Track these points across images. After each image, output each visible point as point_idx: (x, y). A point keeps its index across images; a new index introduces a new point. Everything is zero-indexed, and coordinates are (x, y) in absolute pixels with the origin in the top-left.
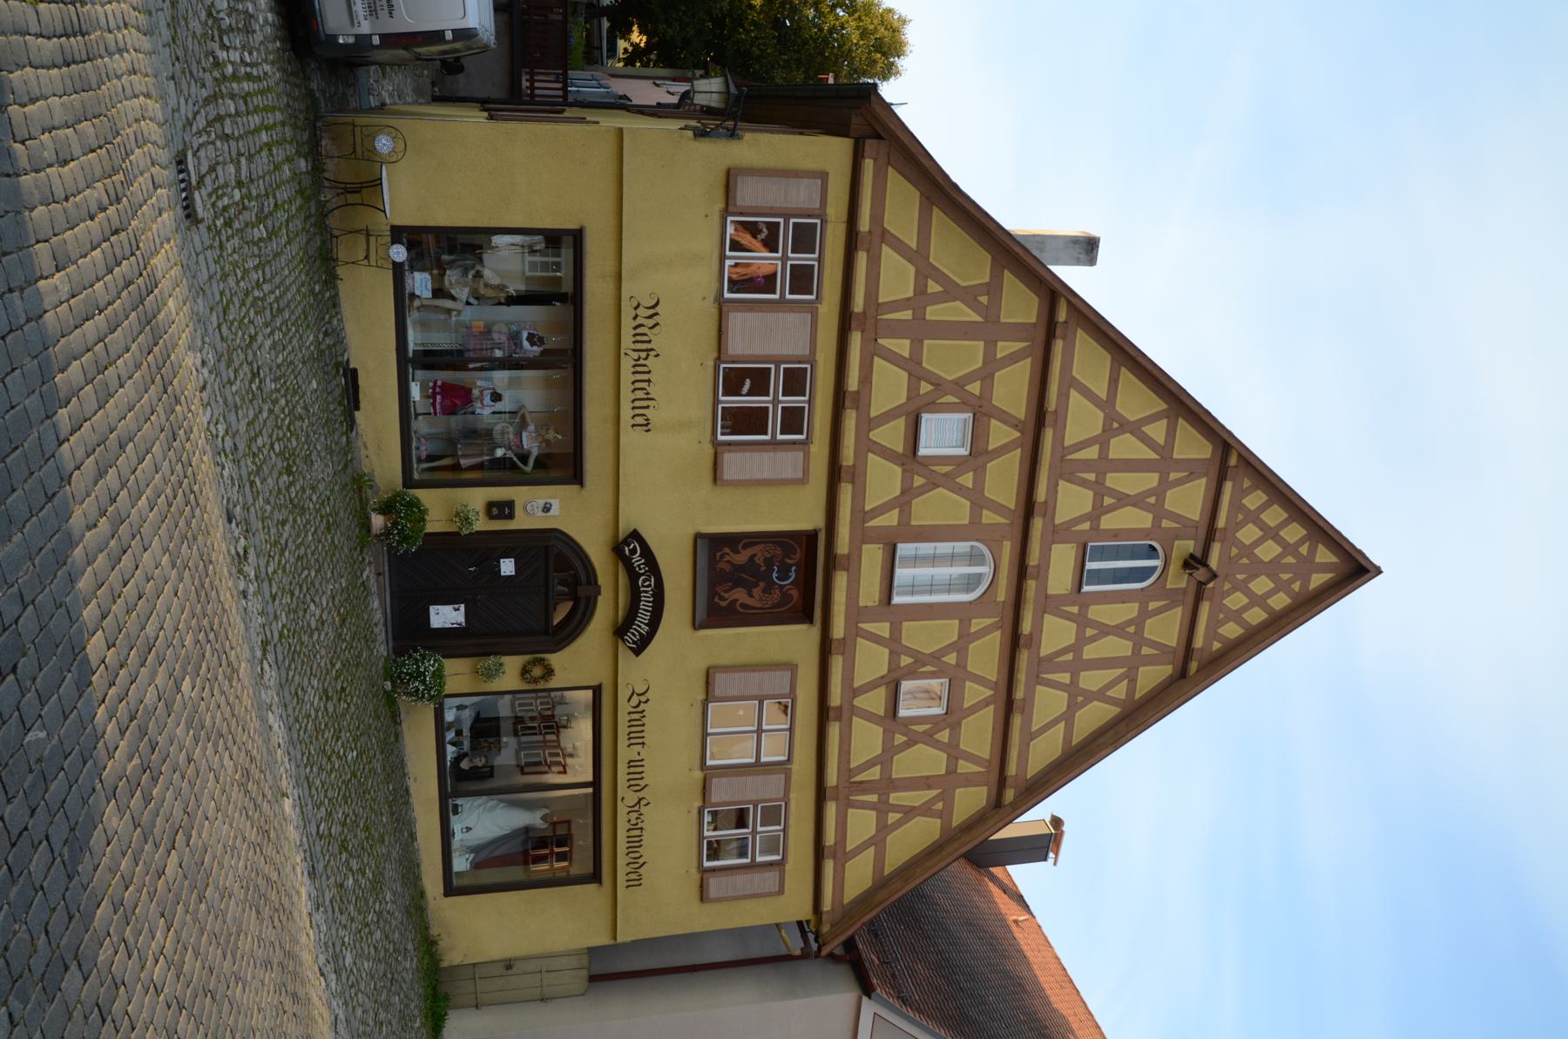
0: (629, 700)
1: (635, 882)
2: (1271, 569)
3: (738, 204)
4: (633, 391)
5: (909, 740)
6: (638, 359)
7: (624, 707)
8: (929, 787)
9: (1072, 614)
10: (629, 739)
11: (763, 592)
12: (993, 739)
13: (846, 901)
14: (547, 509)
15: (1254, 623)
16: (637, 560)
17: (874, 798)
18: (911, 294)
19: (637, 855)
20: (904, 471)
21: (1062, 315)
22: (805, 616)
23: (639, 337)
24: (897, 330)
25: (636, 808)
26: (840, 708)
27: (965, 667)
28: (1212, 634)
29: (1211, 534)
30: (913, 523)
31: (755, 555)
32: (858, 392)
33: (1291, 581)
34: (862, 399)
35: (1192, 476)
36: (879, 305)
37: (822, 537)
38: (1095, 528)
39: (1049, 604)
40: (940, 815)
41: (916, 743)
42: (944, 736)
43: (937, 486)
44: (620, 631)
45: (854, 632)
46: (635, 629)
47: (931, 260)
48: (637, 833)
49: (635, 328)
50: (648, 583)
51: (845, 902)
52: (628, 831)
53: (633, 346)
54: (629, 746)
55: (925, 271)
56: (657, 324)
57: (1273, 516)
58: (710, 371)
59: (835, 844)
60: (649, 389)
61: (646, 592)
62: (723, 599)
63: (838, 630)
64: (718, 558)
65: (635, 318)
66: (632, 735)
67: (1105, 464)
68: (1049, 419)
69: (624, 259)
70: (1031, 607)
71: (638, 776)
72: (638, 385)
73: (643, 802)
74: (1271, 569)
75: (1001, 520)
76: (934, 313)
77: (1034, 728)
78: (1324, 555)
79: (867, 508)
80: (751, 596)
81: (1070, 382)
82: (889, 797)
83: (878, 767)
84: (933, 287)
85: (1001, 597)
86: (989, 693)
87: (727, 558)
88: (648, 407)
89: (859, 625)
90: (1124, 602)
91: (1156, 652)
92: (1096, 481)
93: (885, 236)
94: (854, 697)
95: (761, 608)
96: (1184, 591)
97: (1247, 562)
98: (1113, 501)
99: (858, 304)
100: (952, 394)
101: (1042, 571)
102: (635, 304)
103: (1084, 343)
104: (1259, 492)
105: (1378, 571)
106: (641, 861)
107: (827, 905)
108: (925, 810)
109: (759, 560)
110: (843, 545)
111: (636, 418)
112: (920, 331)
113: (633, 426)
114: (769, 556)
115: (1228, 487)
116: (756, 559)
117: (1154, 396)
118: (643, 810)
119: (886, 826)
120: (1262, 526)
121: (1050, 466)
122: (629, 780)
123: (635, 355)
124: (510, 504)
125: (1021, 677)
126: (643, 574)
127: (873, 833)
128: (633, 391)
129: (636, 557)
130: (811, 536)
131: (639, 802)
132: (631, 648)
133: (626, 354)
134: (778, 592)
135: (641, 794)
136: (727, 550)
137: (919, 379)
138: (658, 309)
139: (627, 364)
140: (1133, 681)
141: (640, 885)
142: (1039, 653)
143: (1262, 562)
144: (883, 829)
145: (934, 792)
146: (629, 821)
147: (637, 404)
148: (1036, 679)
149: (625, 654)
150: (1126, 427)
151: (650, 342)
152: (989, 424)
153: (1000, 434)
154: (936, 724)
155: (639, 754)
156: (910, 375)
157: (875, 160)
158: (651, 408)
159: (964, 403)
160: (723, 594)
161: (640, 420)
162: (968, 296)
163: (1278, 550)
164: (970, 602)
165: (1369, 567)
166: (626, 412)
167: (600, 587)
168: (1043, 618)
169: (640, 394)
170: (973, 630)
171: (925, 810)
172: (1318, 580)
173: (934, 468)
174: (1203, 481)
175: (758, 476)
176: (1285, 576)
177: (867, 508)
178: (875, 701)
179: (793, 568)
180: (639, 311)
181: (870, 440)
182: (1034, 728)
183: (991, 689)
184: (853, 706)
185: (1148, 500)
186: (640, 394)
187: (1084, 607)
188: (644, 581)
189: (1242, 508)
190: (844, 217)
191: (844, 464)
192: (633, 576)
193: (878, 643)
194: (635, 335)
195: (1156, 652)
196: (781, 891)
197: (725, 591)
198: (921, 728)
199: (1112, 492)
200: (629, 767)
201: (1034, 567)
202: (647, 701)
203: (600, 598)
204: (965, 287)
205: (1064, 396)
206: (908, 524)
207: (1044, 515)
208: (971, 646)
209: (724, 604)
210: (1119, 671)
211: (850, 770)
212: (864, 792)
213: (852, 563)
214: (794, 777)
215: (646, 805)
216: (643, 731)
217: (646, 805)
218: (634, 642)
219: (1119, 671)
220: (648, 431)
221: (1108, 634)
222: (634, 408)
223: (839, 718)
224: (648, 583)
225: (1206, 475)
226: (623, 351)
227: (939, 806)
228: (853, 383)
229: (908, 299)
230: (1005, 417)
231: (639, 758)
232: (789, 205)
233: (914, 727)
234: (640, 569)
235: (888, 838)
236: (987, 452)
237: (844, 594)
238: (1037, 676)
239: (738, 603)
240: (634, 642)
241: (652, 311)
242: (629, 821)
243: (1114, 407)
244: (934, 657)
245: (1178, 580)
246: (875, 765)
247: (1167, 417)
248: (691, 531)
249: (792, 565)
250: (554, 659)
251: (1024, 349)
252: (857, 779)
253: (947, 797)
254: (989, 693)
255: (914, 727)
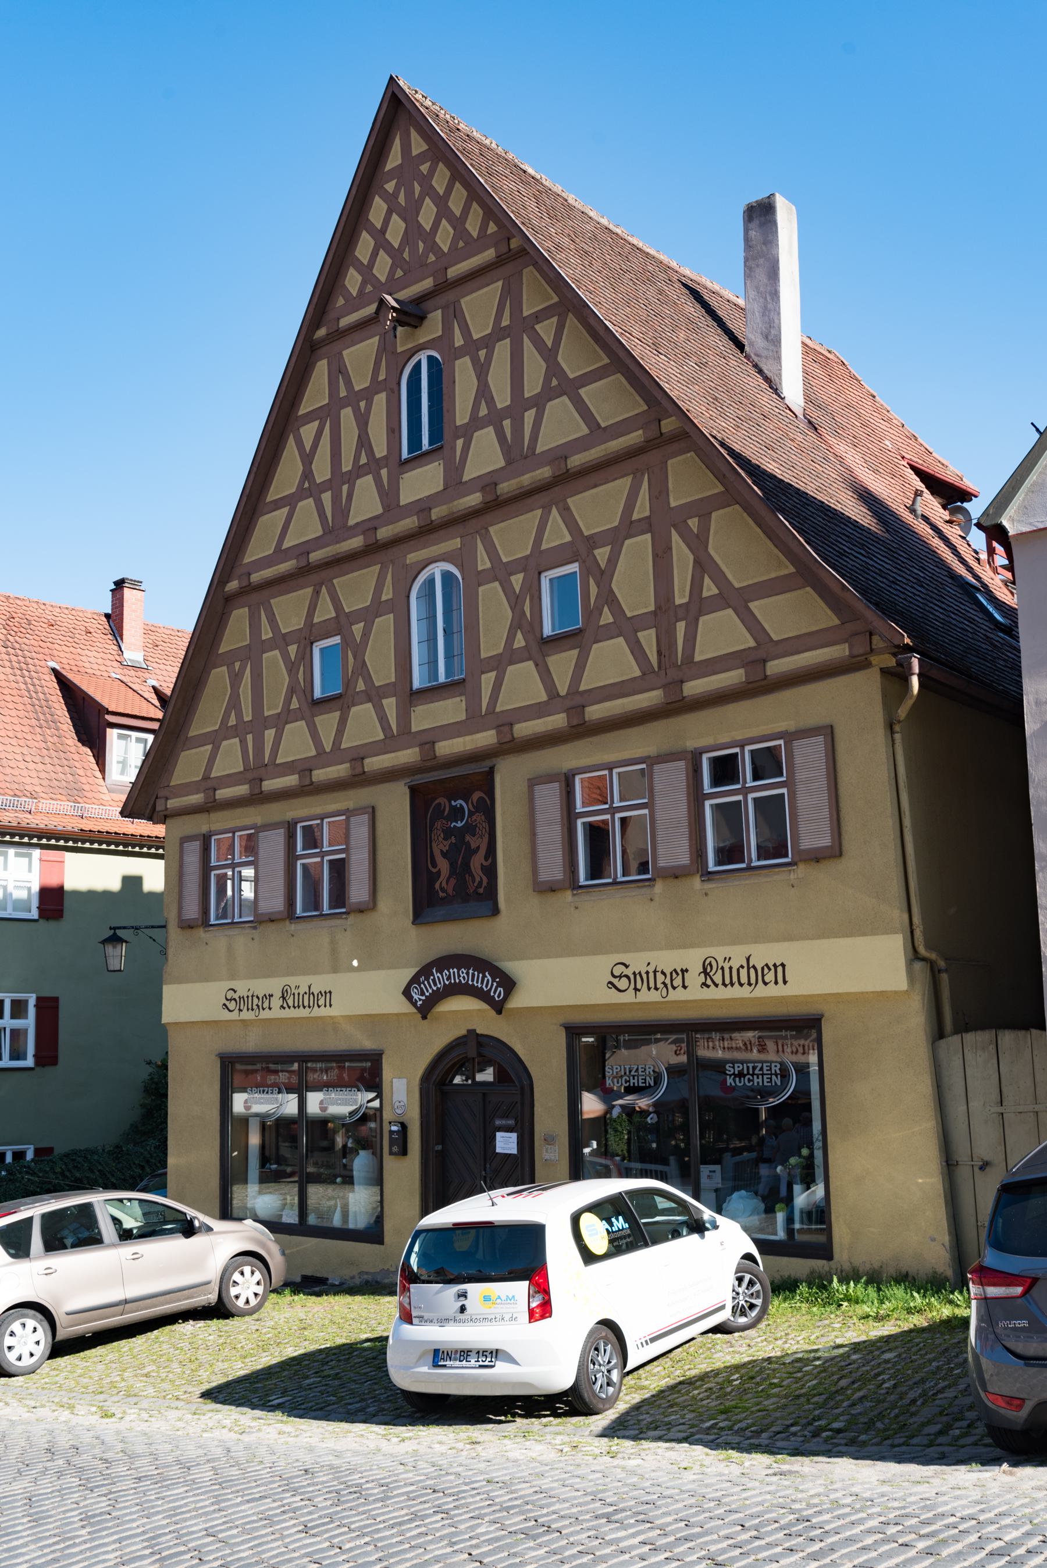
20: (354, 705)
36: (245, 770)
37: (420, 779)
62: (481, 882)
63: (486, 738)
80: (478, 848)
81: (280, 554)
82: (680, 605)
85: (456, 543)
87: (444, 884)
93: (206, 778)
96: (444, 308)
108: (698, 543)
110: (408, 756)
121: (338, 542)
134: (474, 817)
145: (675, 537)
149: (516, 1002)
157: (167, 799)
171: (698, 543)
179: (453, 803)
183: (550, 512)
197: (474, 881)
198: (594, 590)
206: (394, 684)
212: (673, 643)
213: (427, 741)
239: (485, 863)
248: (413, 931)
252: (653, 658)
253: (678, 519)
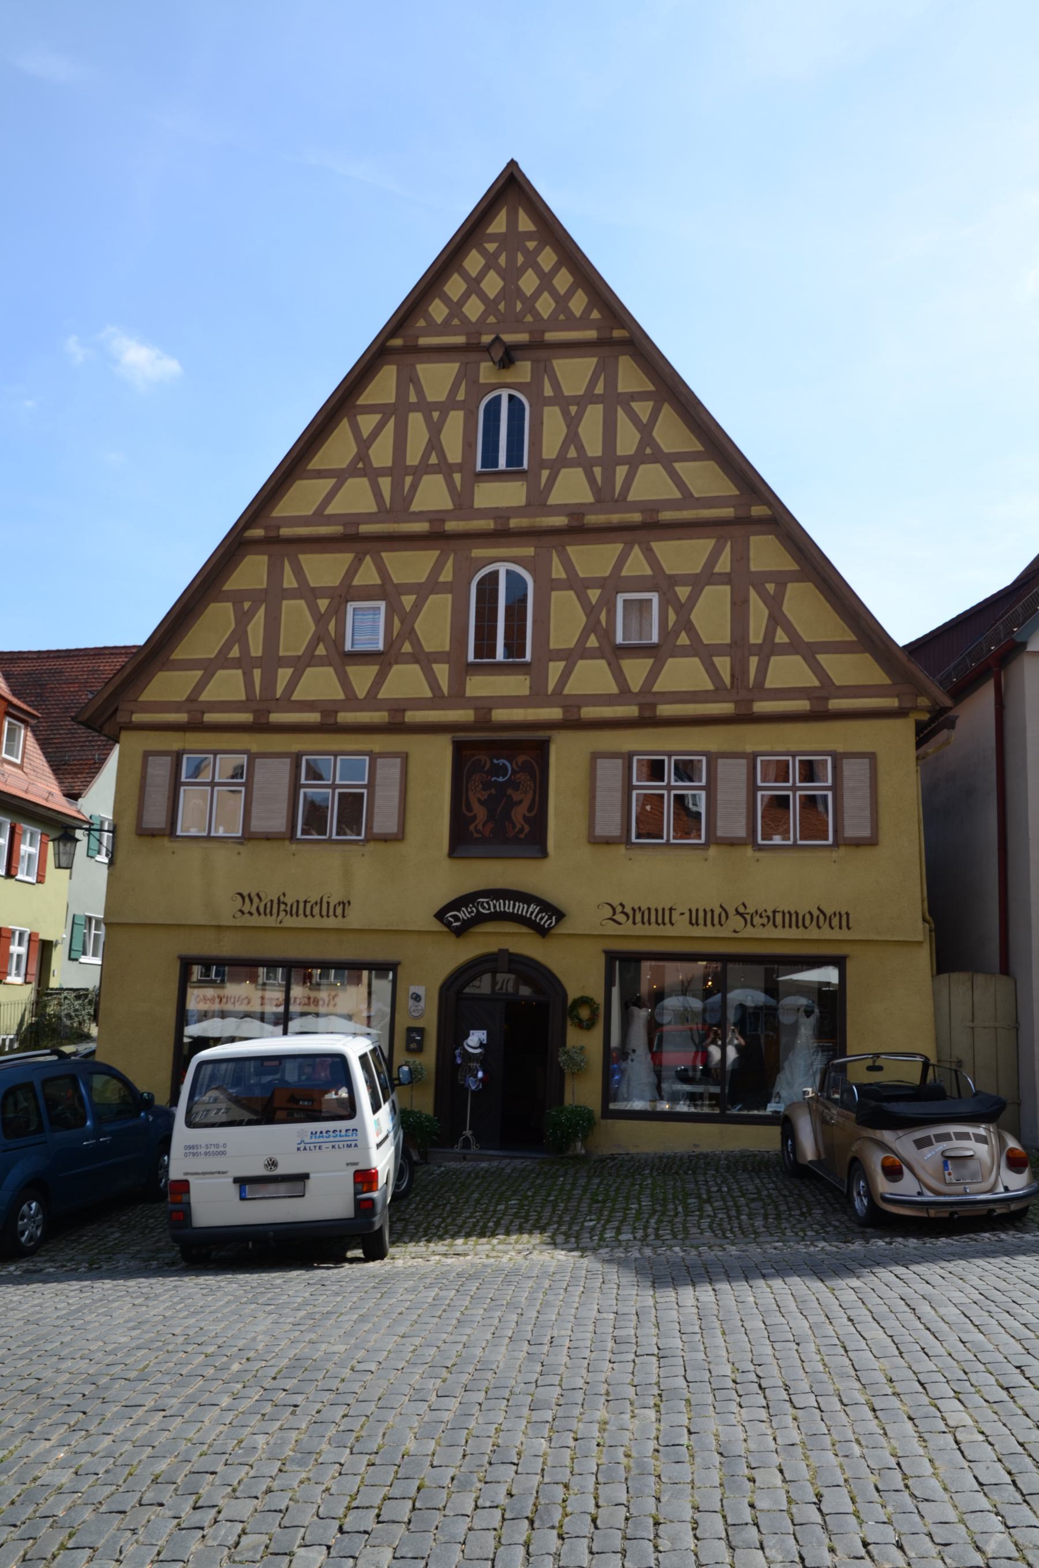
0: (619, 923)
1: (844, 920)
2: (511, 276)
3: (164, 826)
4: (313, 916)
5: (685, 629)
6: (285, 911)
7: (627, 928)
8: (746, 601)
9: (550, 475)
10: (664, 924)
11: (517, 790)
12: (691, 538)
13: (888, 681)
14: (417, 998)
15: (571, 279)
16: (464, 914)
17: (754, 661)
18: (240, 672)
19: (808, 917)
20: (396, 663)
21: (258, 532)
22: (542, 748)
23: (268, 911)
24: (269, 681)
25: (748, 917)
26: (641, 706)
27: (605, 579)
28: (583, 322)
29: (473, 348)
30: (447, 648)
31: (479, 800)
32: (322, 712)
33: (526, 253)
34: (329, 709)
35: (414, 380)
36: (247, 699)
37: (462, 736)
38: (460, 467)
39: (537, 502)
40: (781, 586)
41: (689, 622)
42: (683, 592)
43: (413, 630)
44: (543, 932)
45: (558, 697)
46: (536, 916)
47: (213, 656)
48: (779, 917)
49: (259, 914)
50: (485, 905)
51: (888, 681)
52: (775, 926)
53: (275, 915)
54: (672, 924)
55: (222, 661)
56: (258, 895)
57: (455, 286)
58: (301, 847)
59: (809, 699)
60: (313, 901)
61: (495, 906)
62: (522, 829)
64: (480, 836)
65: (250, 913)
66: (660, 920)
67: (398, 469)
68: (351, 531)
69: (203, 923)
70: (538, 519)
71: (709, 915)
72: (308, 912)
73: (741, 910)
74: (511, 276)
75: (450, 564)
76: (256, 650)
77: (678, 495)
78: (499, 225)
79: (429, 694)
80: (521, 801)
81: (319, 516)
82: (754, 645)
83: (716, 659)
84: (235, 652)
85: (530, 551)
86: (636, 549)
87: (480, 827)
88: (328, 903)
89: (549, 692)
90: (542, 423)
91: (602, 377)
92: (414, 474)
93: (192, 699)
94: (630, 691)
95: (535, 792)
96: (534, 362)
97: (503, 303)
98: (434, 455)
99: (246, 717)
100: (328, 625)
101: (501, 514)
102: (239, 914)
103: (286, 508)
104: (431, 309)
105: (513, 164)
106: (816, 913)
107: (893, 703)
108: (774, 603)
109: (484, 795)
110: (464, 715)
111: (337, 914)
112: (271, 661)
113: (343, 916)
114: (481, 786)
115: (423, 341)
116: (483, 799)
117: (335, 433)
118: (751, 910)
119: (791, 644)
120: (465, 297)
121: (395, 522)
122: (713, 925)
123: (282, 914)
124: (410, 1030)
125: (616, 518)
126: (477, 909)
127: (798, 658)
128: (313, 916)
129: (461, 915)
130: (460, 749)
131: (741, 915)
132: (557, 921)
133: (280, 922)
134: (518, 776)
135: (731, 912)
136: (472, 828)
137: (313, 656)
138: (245, 894)
139: (290, 922)
140: (634, 397)
141: (847, 914)
142: (591, 504)
143: (504, 288)
144: (796, 646)
145: (753, 595)
146: (763, 925)
147: (324, 913)
148: (621, 502)
149: (563, 929)
150: (362, 455)
151: (272, 901)
152: (357, 586)
153: (368, 575)
154: (668, 602)
155: (682, 914)
156: (309, 665)
157: (132, 713)
158: (329, 900)
159: (336, 613)
160: (516, 830)
161: (339, 911)
162: (243, 619)
163: (492, 274)
164: (535, 582)
165: (508, 174)
166: (331, 922)
167: (500, 951)
168: (551, 506)
169: (316, 910)
170: (563, 576)
171: (774, 603)
172: (525, 223)
173: (395, 634)
174: (420, 367)
175: (396, 800)
176: (520, 259)
177: (429, 694)
178: (636, 670)
179: (495, 761)
180: (246, 911)
181: (365, 698)
182: (678, 495)
183: (632, 548)
184: (640, 692)
185: (435, 420)
186: (316, 910)
187: (542, 464)
188: (484, 908)
189: (447, 321)
190: (180, 734)
191: (387, 720)
192: (480, 919)
193: (570, 673)
194: (265, 914)
195: (602, 377)
196: (872, 757)
197: (514, 826)
198: (672, 617)
199: (426, 456)
200: (697, 924)
201: (495, 523)
202: (622, 905)
203: (511, 950)
204: (236, 624)
205: (331, 520)
206: (448, 654)
207: (443, 521)
208: (581, 575)
209: (527, 828)
210: (620, 413)
211: (717, 689)
212: (745, 671)
213: (484, 706)
214: (726, 748)
215: (745, 907)
216: (656, 910)
217: (745, 907)
218: (550, 918)
219: (620, 413)
220: (349, 903)
221: (576, 434)
222: (328, 916)
223: (653, 706)
224: (485, 905)
225: (413, 366)
226: (278, 925)
227: (771, 587)
228: (314, 717)
229: (244, 673)
230: (352, 572)
231: (687, 914)
232: (168, 782)
233: (671, 624)
234: (472, 912)
235: (806, 640)
236: (382, 585)
237: (515, 711)
238: (617, 501)
239: (527, 814)
240: (550, 918)
241: (247, 899)
242: (763, 925)
243: (343, 469)
244: (591, 611)
245: (523, 371)
246: (713, 664)
247: (355, 416)
248: (446, 863)
249: (492, 762)
250: (573, 993)
251: (290, 563)
252: (727, 680)
253: (758, 581)
254: (636, 549)
255: (671, 624)
